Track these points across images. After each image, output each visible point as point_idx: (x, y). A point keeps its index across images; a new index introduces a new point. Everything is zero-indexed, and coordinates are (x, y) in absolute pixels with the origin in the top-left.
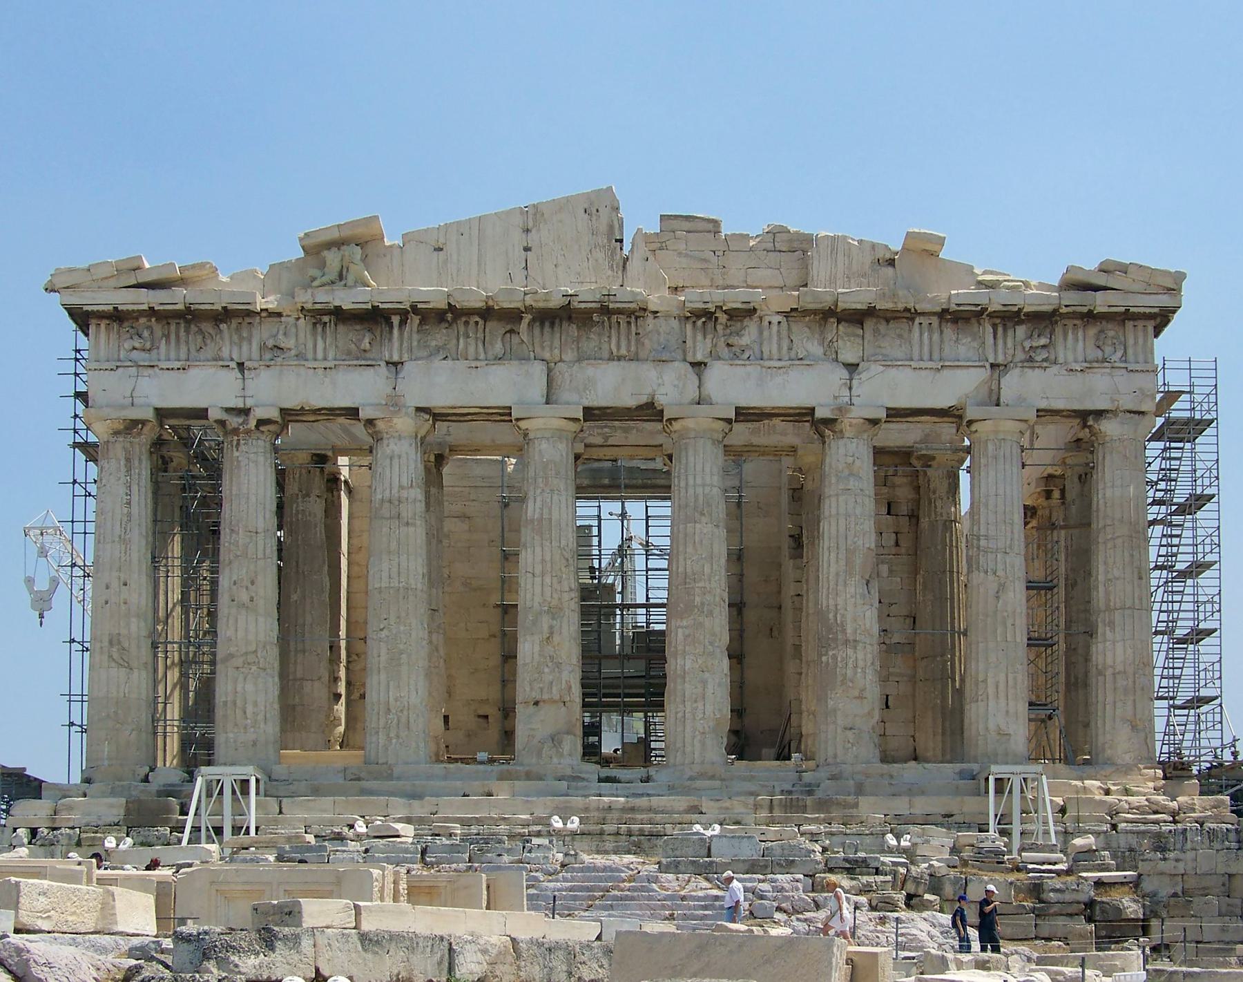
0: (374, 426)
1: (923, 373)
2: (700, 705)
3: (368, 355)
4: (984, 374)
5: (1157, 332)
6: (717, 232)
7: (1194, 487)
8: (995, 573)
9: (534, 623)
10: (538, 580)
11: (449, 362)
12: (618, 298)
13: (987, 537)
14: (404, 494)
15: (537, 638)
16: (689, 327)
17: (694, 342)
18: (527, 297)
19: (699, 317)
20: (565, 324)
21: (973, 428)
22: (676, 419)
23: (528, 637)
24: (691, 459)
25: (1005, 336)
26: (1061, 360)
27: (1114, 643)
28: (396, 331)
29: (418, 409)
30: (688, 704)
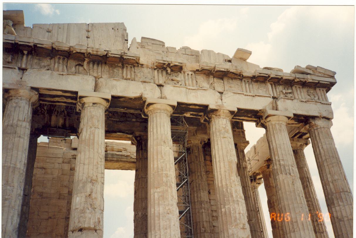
0: (9, 93)
1: (249, 97)
2: (168, 231)
3: (9, 64)
4: (271, 100)
5: (327, 91)
6: (164, 46)
7: (328, 159)
8: (290, 174)
9: (84, 187)
10: (86, 167)
11: (50, 71)
12: (128, 54)
13: (283, 160)
14: (20, 123)
15: (83, 195)
16: (156, 71)
17: (158, 78)
18: (88, 49)
19: (160, 69)
20: (103, 65)
21: (269, 119)
22: (150, 104)
23: (79, 195)
24: (158, 120)
25: (276, 89)
26: (297, 97)
27: (344, 206)
28: (25, 57)
29: (33, 88)
30: (162, 231)
